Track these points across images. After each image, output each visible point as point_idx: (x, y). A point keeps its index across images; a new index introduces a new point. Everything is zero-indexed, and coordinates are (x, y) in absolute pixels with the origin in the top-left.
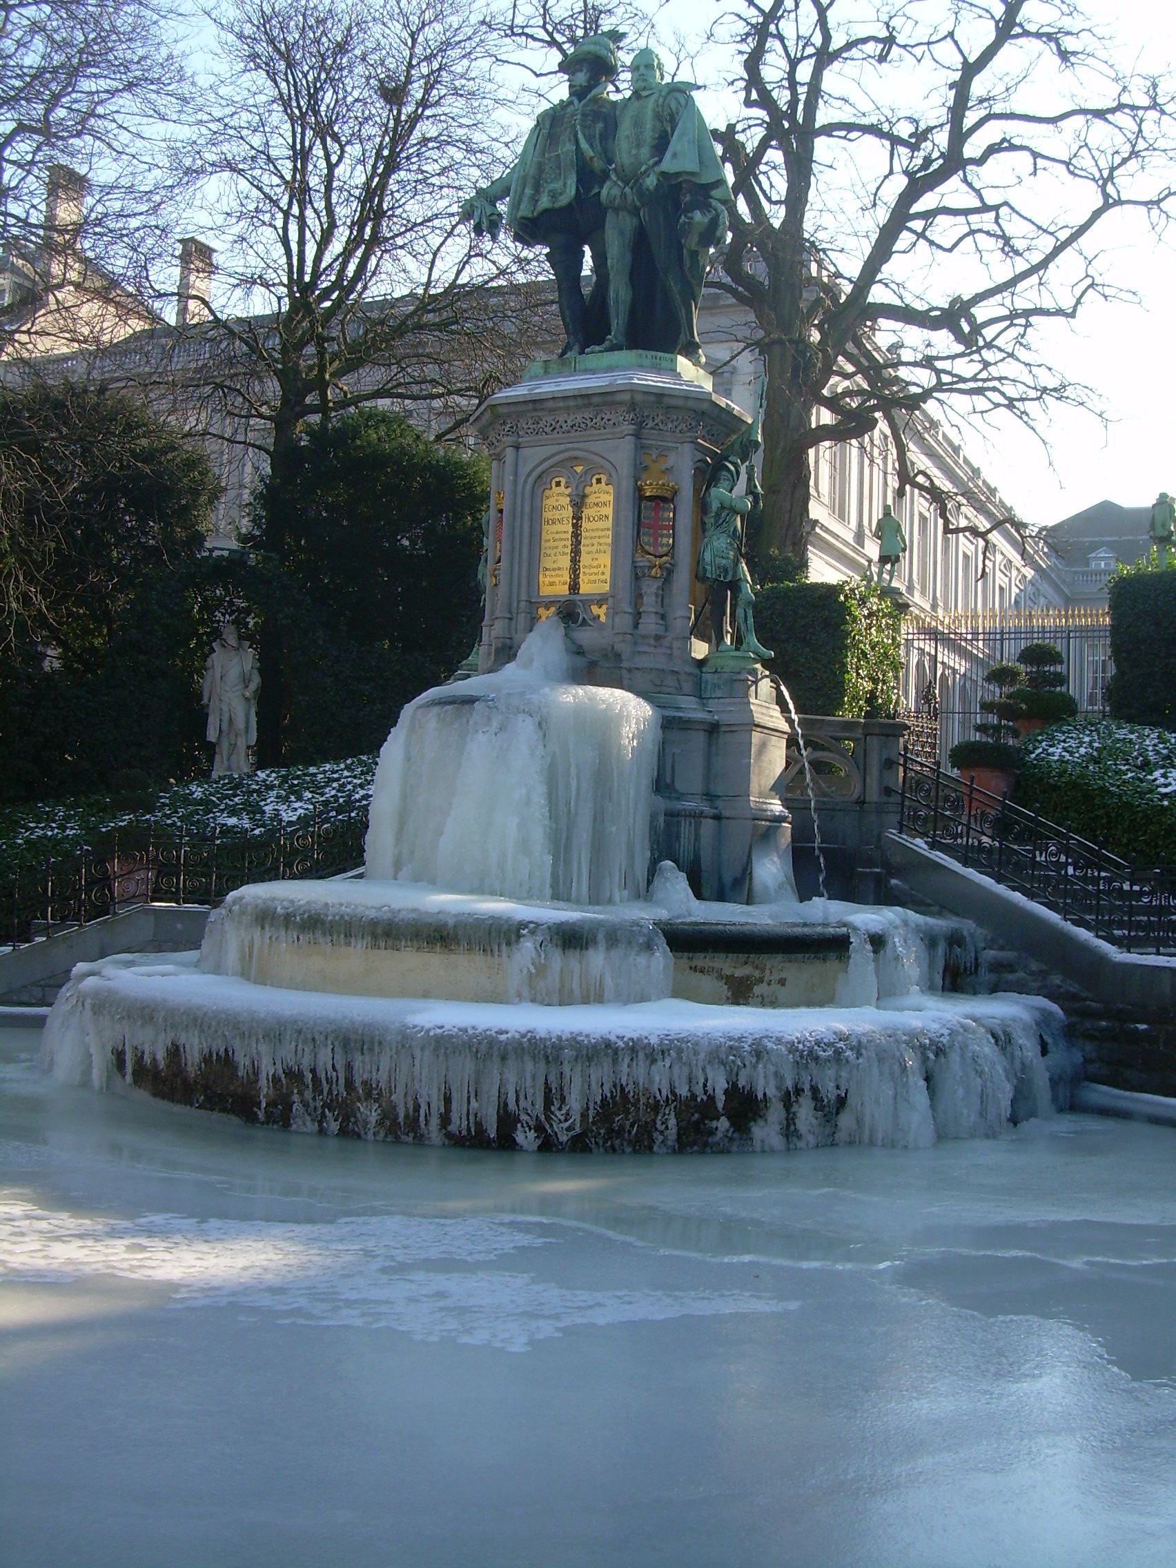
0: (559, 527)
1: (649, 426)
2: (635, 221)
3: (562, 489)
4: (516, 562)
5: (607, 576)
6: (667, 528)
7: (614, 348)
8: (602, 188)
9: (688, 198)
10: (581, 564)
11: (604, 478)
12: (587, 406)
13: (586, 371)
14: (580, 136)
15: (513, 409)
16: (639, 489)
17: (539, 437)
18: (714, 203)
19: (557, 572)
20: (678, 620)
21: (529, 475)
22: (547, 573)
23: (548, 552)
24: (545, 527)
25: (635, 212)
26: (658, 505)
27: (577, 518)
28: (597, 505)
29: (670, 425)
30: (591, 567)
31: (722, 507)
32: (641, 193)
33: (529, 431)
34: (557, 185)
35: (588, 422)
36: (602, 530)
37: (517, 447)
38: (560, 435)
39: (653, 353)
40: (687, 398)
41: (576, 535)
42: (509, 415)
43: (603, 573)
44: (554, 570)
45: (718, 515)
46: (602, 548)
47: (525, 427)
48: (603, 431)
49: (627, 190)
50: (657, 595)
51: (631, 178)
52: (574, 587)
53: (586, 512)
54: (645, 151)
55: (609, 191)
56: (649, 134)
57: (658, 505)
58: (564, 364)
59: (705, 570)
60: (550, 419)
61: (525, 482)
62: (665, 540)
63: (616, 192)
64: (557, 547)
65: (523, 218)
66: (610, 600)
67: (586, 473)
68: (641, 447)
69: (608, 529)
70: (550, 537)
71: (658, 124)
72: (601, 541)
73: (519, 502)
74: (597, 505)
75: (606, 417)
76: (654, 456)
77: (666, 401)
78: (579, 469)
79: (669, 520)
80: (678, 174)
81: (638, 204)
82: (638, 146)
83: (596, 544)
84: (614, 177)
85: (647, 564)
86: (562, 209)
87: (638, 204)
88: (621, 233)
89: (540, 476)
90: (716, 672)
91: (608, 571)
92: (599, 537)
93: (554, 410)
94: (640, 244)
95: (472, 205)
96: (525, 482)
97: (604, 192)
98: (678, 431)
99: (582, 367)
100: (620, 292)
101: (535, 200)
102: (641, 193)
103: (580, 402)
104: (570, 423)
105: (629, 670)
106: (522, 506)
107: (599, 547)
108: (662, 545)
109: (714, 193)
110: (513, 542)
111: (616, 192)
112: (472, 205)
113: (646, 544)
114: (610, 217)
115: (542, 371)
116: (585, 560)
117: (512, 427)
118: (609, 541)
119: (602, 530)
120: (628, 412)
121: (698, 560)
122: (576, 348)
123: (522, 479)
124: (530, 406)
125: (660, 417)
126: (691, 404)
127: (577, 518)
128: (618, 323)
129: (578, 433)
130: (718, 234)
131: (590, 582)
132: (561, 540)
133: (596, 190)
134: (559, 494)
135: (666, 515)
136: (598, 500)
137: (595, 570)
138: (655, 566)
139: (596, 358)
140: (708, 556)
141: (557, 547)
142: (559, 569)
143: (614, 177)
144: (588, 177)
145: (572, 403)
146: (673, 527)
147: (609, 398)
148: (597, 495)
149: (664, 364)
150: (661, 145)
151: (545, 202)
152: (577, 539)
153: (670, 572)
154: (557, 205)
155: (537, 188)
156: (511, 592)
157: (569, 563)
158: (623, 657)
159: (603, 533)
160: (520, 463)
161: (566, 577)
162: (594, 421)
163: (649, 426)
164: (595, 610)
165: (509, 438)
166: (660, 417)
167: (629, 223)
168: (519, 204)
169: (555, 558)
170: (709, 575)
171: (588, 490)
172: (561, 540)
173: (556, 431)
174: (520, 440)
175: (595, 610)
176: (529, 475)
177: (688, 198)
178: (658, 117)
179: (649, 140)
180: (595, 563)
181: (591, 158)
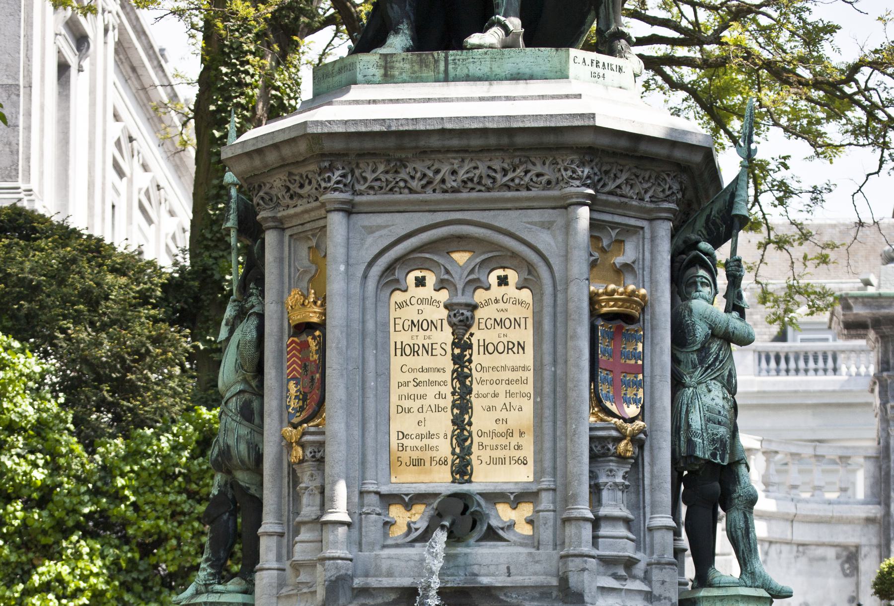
0: (424, 360)
1: (607, 189)
3: (427, 292)
10: (474, 429)
13: (468, 78)
16: (593, 299)
17: (397, 197)
19: (426, 441)
20: (658, 535)
22: (406, 442)
23: (406, 404)
24: (396, 362)
26: (619, 328)
28: (500, 323)
33: (377, 184)
35: (498, 176)
36: (513, 369)
37: (350, 210)
38: (439, 196)
43: (519, 447)
44: (420, 437)
46: (516, 402)
47: (370, 177)
48: (524, 193)
53: (478, 335)
57: (619, 328)
59: (691, 444)
60: (421, 167)
61: (365, 276)
62: (630, 394)
64: (423, 397)
69: (524, 368)
70: (409, 377)
72: (514, 388)
73: (356, 315)
74: (500, 323)
75: (539, 169)
77: (643, 147)
78: (461, 258)
79: (637, 356)
83: (502, 395)
85: (614, 433)
89: (390, 268)
92: (509, 382)
93: (438, 151)
96: (365, 276)
98: (647, 198)
99: (461, 71)
104: (462, 175)
107: (509, 400)
108: (628, 403)
113: (607, 398)
115: (379, 73)
117: (344, 176)
118: (529, 388)
119: (513, 369)
120: (582, 164)
121: (679, 426)
126: (678, 154)
129: (474, 195)
131: (493, 461)
132: (431, 383)
134: (422, 301)
135: (630, 349)
136: (504, 316)
137: (503, 441)
138: (624, 437)
140: (696, 420)
141: (423, 397)
142: (430, 436)
146: (642, 369)
148: (501, 305)
152: (463, 384)
157: (450, 427)
158: (586, 599)
161: (444, 448)
162: (510, 175)
163: (607, 189)
164: (504, 513)
165: (337, 195)
169: (421, 417)
170: (699, 453)
171: (480, 296)
172: (431, 383)
173: (429, 189)
174: (358, 199)
175: (504, 513)
180: (501, 428)
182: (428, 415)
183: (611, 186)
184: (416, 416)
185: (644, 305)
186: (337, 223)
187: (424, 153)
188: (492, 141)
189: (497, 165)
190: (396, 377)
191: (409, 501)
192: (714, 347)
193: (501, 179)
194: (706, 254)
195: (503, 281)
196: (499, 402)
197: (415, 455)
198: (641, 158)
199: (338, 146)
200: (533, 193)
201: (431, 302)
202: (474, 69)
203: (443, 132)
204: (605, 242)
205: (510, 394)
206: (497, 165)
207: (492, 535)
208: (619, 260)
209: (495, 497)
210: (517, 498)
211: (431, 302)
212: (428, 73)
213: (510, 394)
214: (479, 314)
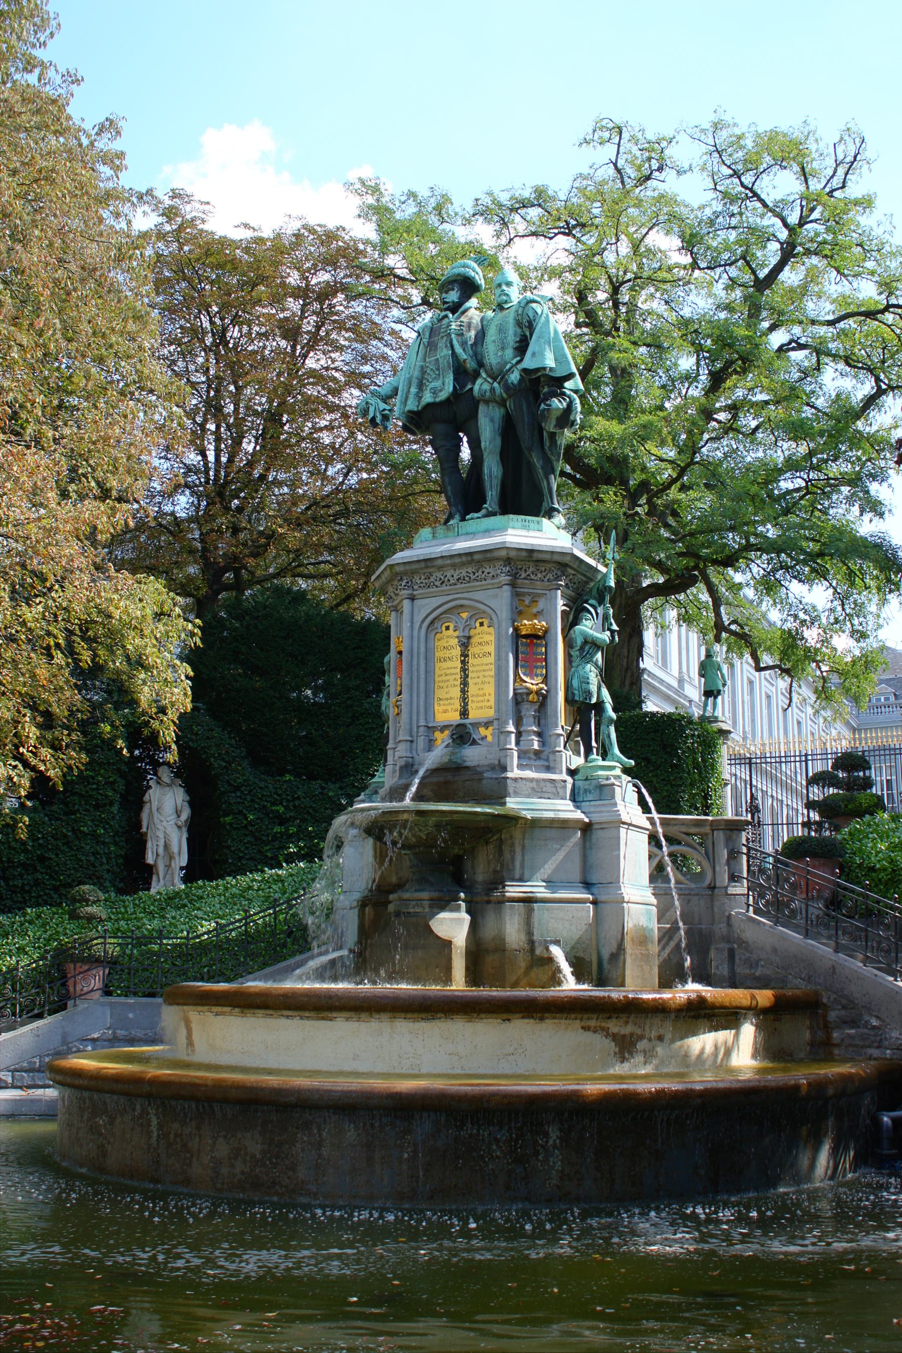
0: (449, 664)
2: (503, 410)
3: (451, 632)
4: (415, 695)
5: (492, 703)
6: (541, 660)
7: (490, 514)
8: (474, 384)
9: (546, 390)
11: (486, 622)
12: (470, 563)
14: (455, 342)
15: (408, 567)
16: (516, 630)
18: (568, 392)
21: (423, 621)
24: (438, 665)
25: (502, 403)
26: (532, 642)
27: (465, 655)
28: (480, 644)
29: (539, 575)
30: (478, 695)
31: (586, 642)
32: (507, 387)
34: (437, 384)
37: (412, 598)
39: (523, 517)
40: (552, 552)
41: (464, 670)
42: (405, 573)
45: (582, 648)
46: (487, 680)
48: (484, 582)
49: (496, 385)
50: (534, 717)
51: (498, 375)
52: (464, 713)
53: (472, 650)
54: (509, 352)
55: (481, 386)
56: (512, 338)
57: (532, 642)
58: (448, 529)
59: (573, 694)
60: (439, 575)
61: (420, 627)
62: (539, 671)
63: (486, 387)
65: (410, 412)
66: (495, 722)
67: (471, 617)
68: (517, 595)
70: (443, 672)
71: (519, 331)
72: (486, 673)
73: (415, 646)
74: (480, 644)
76: (527, 602)
77: (535, 555)
78: (465, 615)
79: (541, 654)
80: (537, 370)
81: (505, 396)
82: (503, 349)
84: (484, 375)
86: (441, 403)
87: (505, 396)
88: (492, 420)
89: (432, 623)
90: (587, 779)
91: (492, 699)
94: (508, 429)
95: (367, 403)
96: (420, 627)
97: (476, 388)
99: (464, 531)
100: (492, 468)
101: (419, 397)
102: (507, 387)
103: (464, 559)
104: (456, 577)
105: (515, 780)
106: (419, 648)
109: (568, 384)
110: (411, 678)
111: (486, 387)
112: (367, 403)
114: (482, 408)
116: (472, 690)
118: (492, 673)
120: (505, 566)
122: (457, 517)
123: (417, 626)
124: (423, 565)
125: (531, 569)
127: (465, 655)
128: (492, 495)
130: (572, 418)
131: (478, 708)
133: (469, 386)
137: (481, 698)
139: (475, 522)
143: (484, 375)
144: (462, 374)
145: (457, 560)
146: (546, 660)
147: (488, 555)
149: (532, 525)
150: (522, 347)
151: (428, 398)
153: (545, 697)
154: (438, 400)
155: (421, 386)
156: (411, 719)
157: (459, 694)
159: (487, 667)
160: (416, 611)
161: (457, 705)
164: (483, 731)
166: (531, 569)
167: (497, 413)
168: (406, 400)
170: (577, 698)
171: (472, 632)
176: (423, 621)
177: (546, 390)
178: (519, 324)
179: (512, 343)
180: (481, 692)
181: (465, 361)
182: (450, 689)
183: (523, 575)
184: (446, 690)
185: (546, 631)
186: (406, 604)
187: (440, 568)
188: (464, 559)
189: (470, 570)
190: (437, 672)
191: (443, 729)
192: (587, 648)
193: (473, 577)
194: (591, 605)
195: (482, 624)
196: (479, 681)
197: (445, 708)
198: (538, 561)
199: (402, 568)
200: (488, 581)
201: (451, 637)
202: (469, 530)
203: (442, 557)
204: (527, 602)
205: (484, 676)
206: (470, 570)
207: (474, 742)
208: (535, 610)
209: (476, 725)
210: (487, 725)
211: (451, 637)
212: (450, 534)
213: (484, 676)
214: (473, 640)
